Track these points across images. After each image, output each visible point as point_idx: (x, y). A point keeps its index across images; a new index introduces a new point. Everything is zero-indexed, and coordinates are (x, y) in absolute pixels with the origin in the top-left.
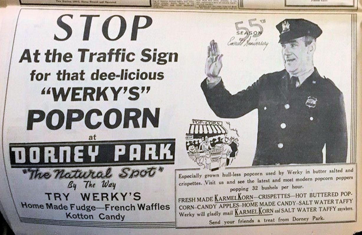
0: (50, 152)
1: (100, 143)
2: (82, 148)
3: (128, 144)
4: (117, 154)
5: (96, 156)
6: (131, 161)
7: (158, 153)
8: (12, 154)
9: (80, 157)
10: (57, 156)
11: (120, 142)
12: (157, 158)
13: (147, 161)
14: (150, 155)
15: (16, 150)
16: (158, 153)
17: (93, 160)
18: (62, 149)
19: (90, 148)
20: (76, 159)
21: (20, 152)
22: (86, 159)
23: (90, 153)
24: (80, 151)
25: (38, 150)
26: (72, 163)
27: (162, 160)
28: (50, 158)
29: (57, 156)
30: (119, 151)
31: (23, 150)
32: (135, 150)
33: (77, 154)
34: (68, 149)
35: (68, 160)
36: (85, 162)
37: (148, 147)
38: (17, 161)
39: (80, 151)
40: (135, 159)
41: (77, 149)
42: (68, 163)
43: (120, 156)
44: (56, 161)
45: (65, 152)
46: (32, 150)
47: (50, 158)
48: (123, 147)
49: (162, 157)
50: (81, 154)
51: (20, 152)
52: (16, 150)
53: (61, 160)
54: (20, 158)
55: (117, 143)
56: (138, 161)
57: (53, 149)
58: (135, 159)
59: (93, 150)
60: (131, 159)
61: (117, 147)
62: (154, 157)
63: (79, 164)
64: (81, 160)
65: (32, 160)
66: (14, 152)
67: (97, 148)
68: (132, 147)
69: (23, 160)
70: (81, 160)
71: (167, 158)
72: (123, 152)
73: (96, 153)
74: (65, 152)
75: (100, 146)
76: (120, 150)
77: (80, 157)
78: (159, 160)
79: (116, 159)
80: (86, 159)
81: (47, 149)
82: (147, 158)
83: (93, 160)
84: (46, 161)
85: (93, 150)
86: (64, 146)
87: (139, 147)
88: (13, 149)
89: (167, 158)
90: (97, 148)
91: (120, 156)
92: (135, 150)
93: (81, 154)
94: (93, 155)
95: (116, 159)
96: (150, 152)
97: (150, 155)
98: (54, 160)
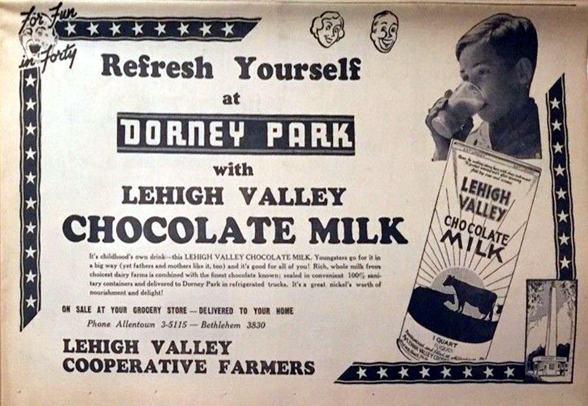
0: (174, 128)
1: (247, 118)
2: (220, 124)
3: (285, 121)
4: (271, 137)
5: (240, 138)
6: (292, 148)
7: (330, 138)
8: (121, 130)
9: (218, 139)
10: (185, 135)
11: (275, 118)
12: (328, 145)
13: (314, 148)
14: (319, 141)
16: (330, 138)
17: (237, 144)
18: (192, 125)
19: (232, 125)
20: (213, 142)
21: (132, 127)
22: (228, 141)
23: (232, 133)
24: (218, 129)
25: (157, 125)
26: (208, 149)
27: (336, 149)
28: (175, 138)
29: (185, 135)
30: (274, 131)
31: (137, 124)
32: (297, 131)
33: (215, 134)
34: (201, 125)
35: (201, 142)
36: (224, 147)
37: (314, 126)
38: (128, 141)
39: (218, 129)
40: (297, 144)
41: (213, 125)
42: (202, 147)
43: (275, 139)
44: (184, 143)
45: (196, 129)
46: (149, 124)
47: (175, 138)
48: (279, 126)
49: (336, 145)
50: (220, 134)
51: (132, 127)
53: (192, 142)
54: (132, 137)
55: (270, 119)
56: (302, 148)
57: (178, 124)
58: (297, 144)
59: (237, 129)
60: (292, 144)
61: (271, 126)
62: (325, 144)
63: (215, 151)
64: (220, 143)
65: (149, 141)
66: (124, 126)
67: (242, 125)
68: (292, 126)
69: (136, 141)
70: (220, 143)
71: (344, 145)
72: (279, 134)
74: (196, 129)
75: (246, 122)
76: (275, 130)
77: (218, 139)
78: (332, 148)
79: (270, 143)
80: (228, 141)
81: (170, 124)
82: (314, 144)
83: (237, 143)
84: (170, 142)
85: (237, 129)
86: (194, 120)
87: (301, 127)
88: (123, 122)
89: (344, 145)
90: (242, 125)
91: (275, 139)
92: (297, 131)
93: (220, 134)
94: (237, 136)
95: (270, 143)
96: (318, 135)
97: (319, 141)
98: (181, 142)
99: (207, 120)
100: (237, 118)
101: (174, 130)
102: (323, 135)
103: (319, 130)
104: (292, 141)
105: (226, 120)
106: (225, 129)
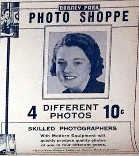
3: (88, 6)
8: (59, 8)
10: (70, 8)
11: (86, 5)
15: (60, 7)
18: (72, 7)
20: (75, 9)
23: (78, 8)
29: (70, 8)
30: (86, 7)
31: (62, 7)
34: (73, 7)
35: (73, 9)
38: (60, 9)
41: (75, 6)
48: (87, 7)
52: (60, 7)
61: (85, 7)
68: (89, 7)
72: (87, 8)
73: (80, 8)
79: (85, 9)
94: (79, 8)
95: (85, 9)
99: (74, 6)
100: (79, 5)
101: (69, 7)
102: (94, 8)
103: (93, 7)
104: (89, 9)
105: (77, 5)
106: (77, 7)
